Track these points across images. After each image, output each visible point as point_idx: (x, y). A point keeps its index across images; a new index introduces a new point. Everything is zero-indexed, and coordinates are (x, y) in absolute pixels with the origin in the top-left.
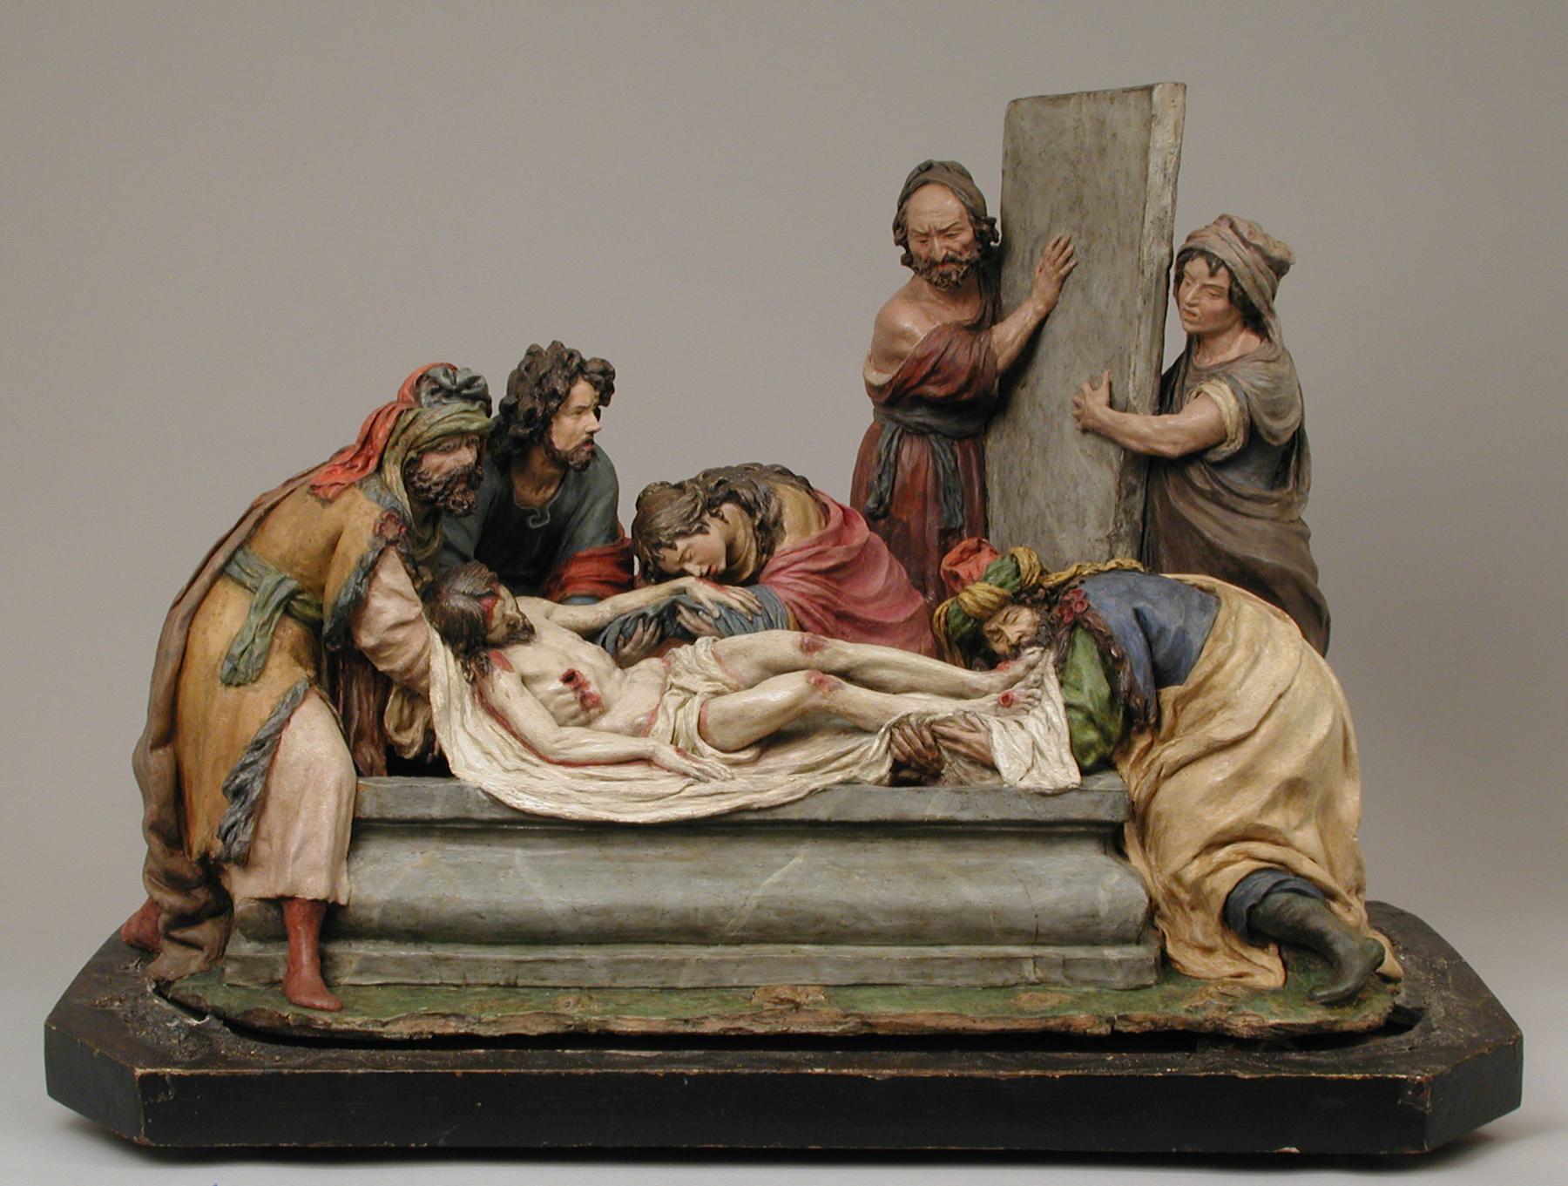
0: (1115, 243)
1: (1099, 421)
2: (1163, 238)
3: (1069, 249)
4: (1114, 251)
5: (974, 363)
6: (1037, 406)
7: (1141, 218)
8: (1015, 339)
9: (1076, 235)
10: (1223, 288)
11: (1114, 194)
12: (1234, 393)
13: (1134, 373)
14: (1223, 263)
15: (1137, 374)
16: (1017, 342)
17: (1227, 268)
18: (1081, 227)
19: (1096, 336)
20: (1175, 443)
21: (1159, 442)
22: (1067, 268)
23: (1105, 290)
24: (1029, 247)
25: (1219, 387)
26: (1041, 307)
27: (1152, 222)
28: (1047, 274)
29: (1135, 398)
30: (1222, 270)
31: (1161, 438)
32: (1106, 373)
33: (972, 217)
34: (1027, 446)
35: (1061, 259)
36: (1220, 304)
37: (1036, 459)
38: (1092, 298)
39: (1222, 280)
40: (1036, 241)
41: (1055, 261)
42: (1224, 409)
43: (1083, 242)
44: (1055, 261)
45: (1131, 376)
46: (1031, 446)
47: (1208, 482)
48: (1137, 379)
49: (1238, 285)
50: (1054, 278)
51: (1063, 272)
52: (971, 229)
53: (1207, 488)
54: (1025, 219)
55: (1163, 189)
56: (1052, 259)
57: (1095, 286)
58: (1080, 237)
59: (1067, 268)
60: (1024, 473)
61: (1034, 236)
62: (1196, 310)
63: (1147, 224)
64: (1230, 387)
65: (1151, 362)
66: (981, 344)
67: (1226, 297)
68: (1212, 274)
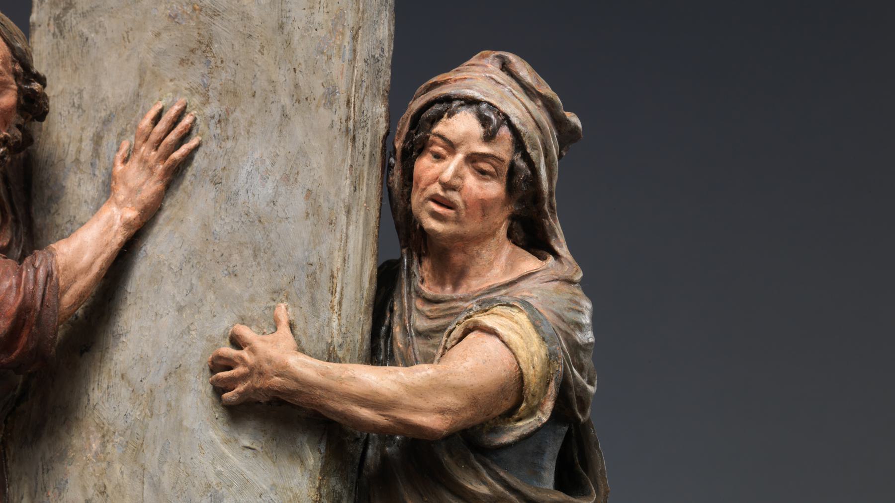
0: (286, 100)
1: (296, 380)
2: (378, 89)
3: (187, 120)
4: (285, 115)
5: (24, 300)
6: (118, 379)
7: (348, 55)
8: (92, 264)
9: (196, 100)
10: (501, 160)
11: (281, 27)
12: (537, 328)
13: (340, 303)
14: (506, 119)
15: (344, 306)
16: (96, 269)
17: (512, 127)
18: (206, 87)
19: (248, 252)
20: (442, 411)
21: (416, 410)
22: (184, 149)
23: (264, 179)
24: (89, 133)
25: (511, 318)
26: (131, 214)
27: (366, 61)
28: (144, 161)
29: (341, 346)
30: (504, 131)
31: (419, 402)
32: (283, 306)
33: (18, 67)
34: (95, 446)
35: (172, 137)
36: (494, 189)
37: (117, 466)
38: (237, 193)
39: (503, 149)
40: (106, 122)
41: (160, 141)
42: (523, 354)
43: (213, 109)
44: (160, 141)
45: (336, 308)
46: (104, 445)
47: (485, 483)
48: (343, 315)
49: (526, 157)
50: (160, 167)
51: (176, 155)
52: (15, 87)
53: (483, 490)
54: (81, 92)
55: (379, 12)
56: (154, 138)
57: (243, 175)
58: (206, 101)
59: (184, 149)
60: (91, 492)
61: (103, 114)
62: (455, 197)
63: (360, 64)
64: (529, 317)
65: (361, 288)
66: (36, 270)
67: (504, 179)
68: (489, 137)
